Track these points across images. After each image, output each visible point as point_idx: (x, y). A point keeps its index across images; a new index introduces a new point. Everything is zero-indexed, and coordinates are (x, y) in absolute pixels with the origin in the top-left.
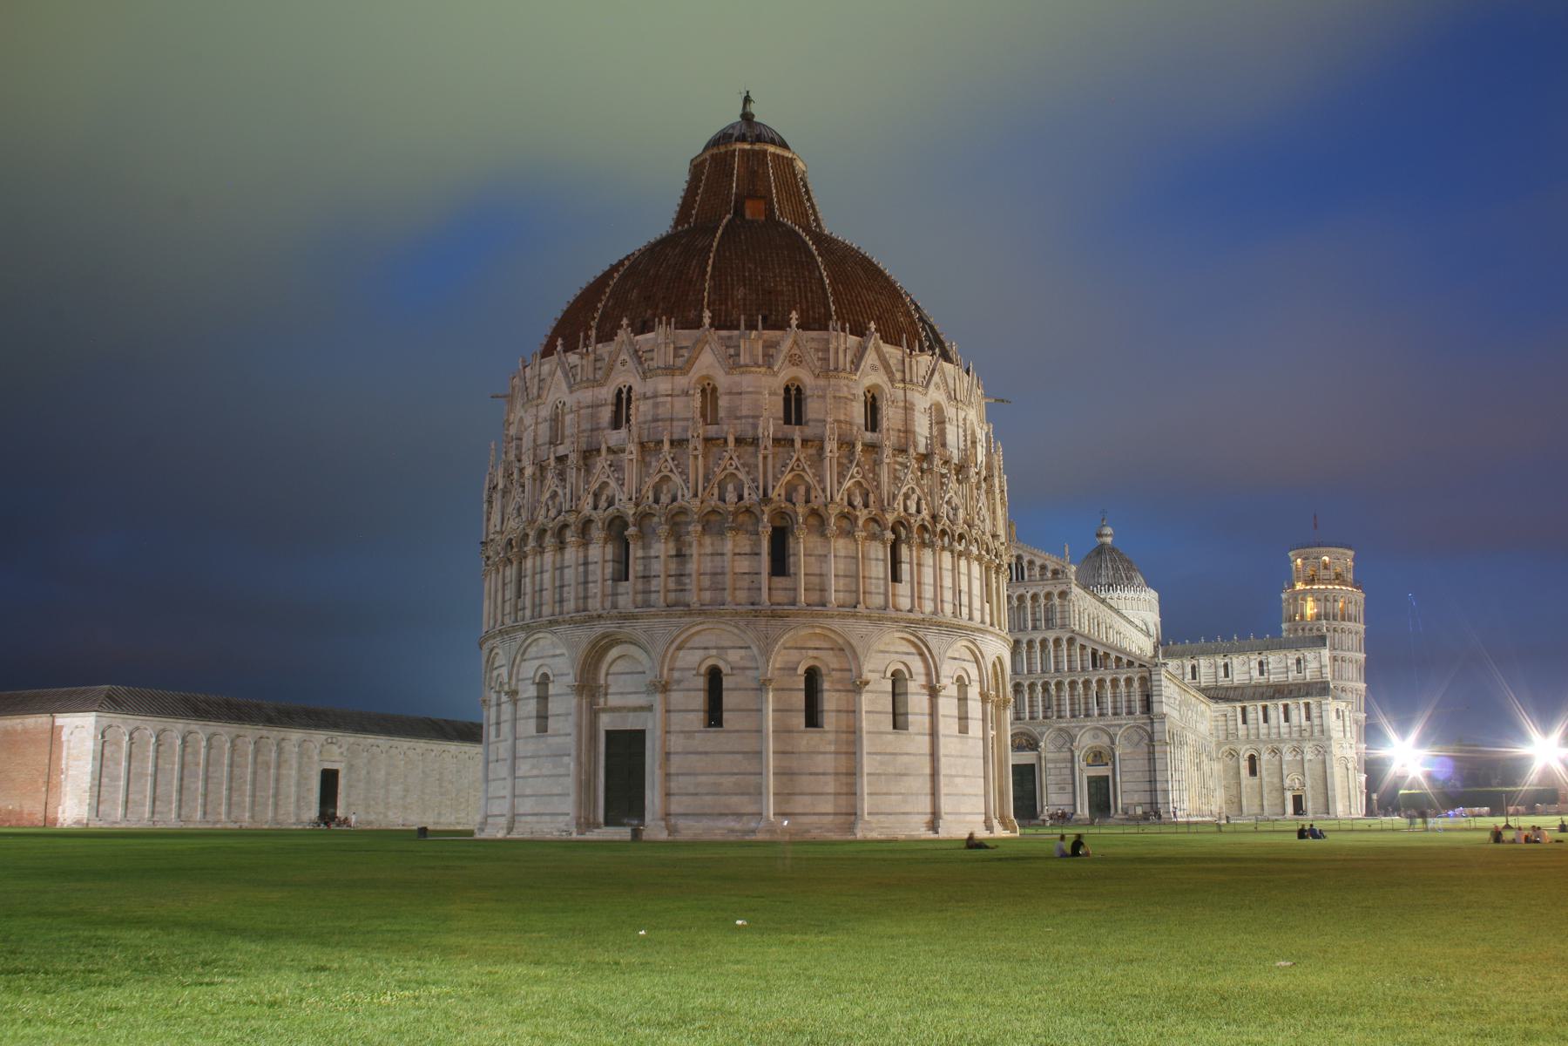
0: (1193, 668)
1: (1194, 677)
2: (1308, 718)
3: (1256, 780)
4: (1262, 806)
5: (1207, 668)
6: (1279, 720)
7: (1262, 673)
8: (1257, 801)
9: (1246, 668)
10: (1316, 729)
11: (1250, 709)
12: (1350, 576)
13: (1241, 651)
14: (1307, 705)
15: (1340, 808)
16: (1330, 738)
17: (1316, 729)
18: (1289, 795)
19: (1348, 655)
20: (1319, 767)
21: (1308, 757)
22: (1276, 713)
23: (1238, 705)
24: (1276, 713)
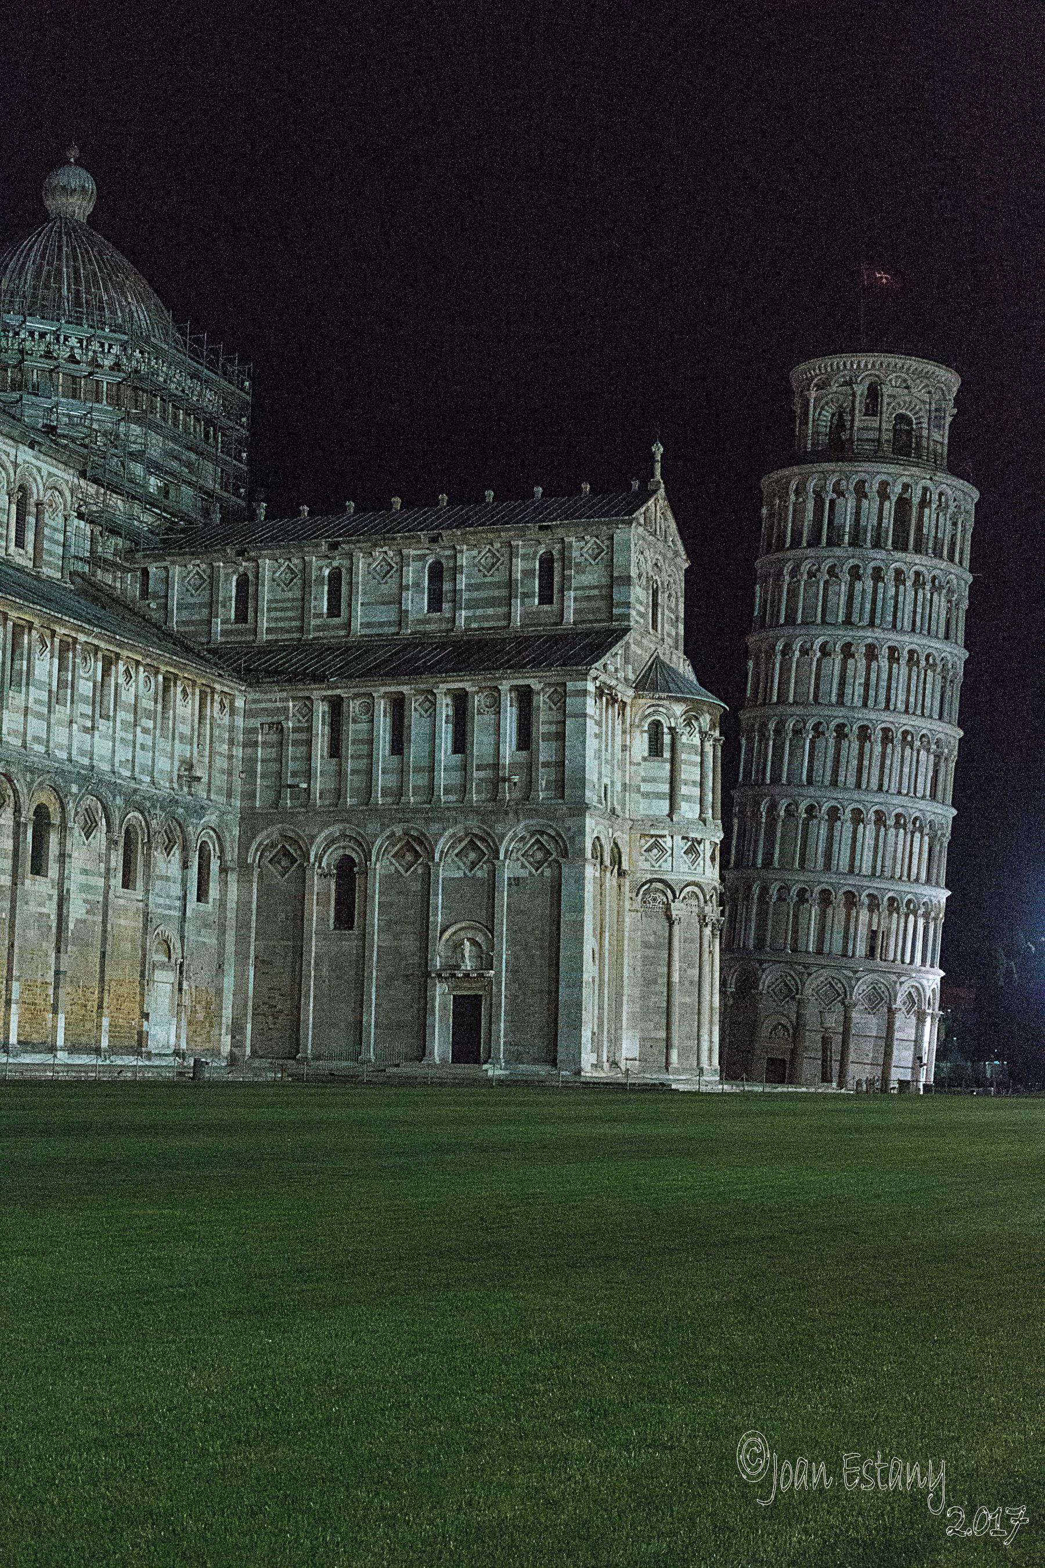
0: (243, 584)
1: (242, 616)
2: (525, 741)
3: (349, 943)
4: (358, 1026)
5: (278, 585)
6: (442, 741)
7: (435, 603)
8: (346, 1012)
9: (389, 587)
10: (543, 778)
11: (354, 707)
12: (941, 437)
13: (379, 528)
14: (525, 697)
15: (609, 1044)
16: (580, 808)
17: (543, 778)
18: (441, 995)
19: (907, 642)
20: (541, 905)
21: (509, 870)
22: (433, 727)
23: (318, 693)
24: (433, 727)
